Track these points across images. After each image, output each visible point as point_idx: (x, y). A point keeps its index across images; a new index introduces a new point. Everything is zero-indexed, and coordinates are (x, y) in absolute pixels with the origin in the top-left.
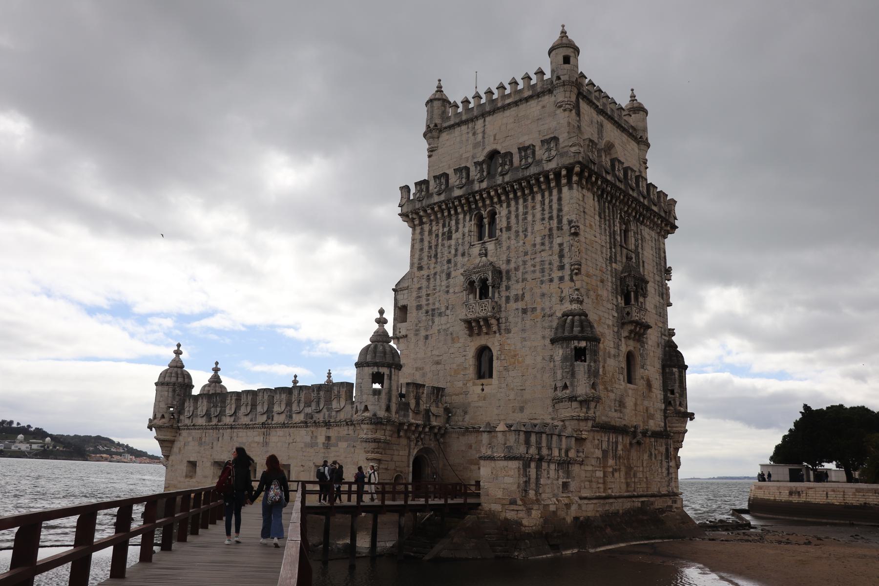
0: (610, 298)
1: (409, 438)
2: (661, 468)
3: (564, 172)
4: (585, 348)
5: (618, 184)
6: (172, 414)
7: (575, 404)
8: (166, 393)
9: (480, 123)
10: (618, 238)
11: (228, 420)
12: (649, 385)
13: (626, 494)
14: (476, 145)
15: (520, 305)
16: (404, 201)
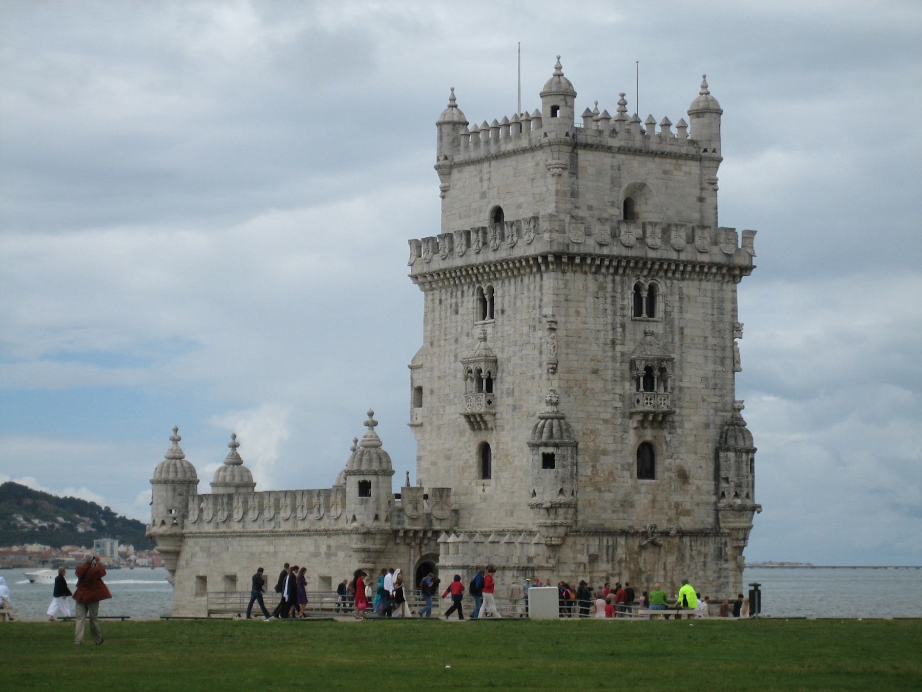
0: (610, 387)
1: (409, 544)
2: (704, 570)
3: (540, 260)
4: (553, 455)
5: (625, 252)
6: (174, 519)
7: (542, 512)
8: (164, 493)
9: (486, 165)
10: (630, 312)
11: (237, 527)
12: (683, 476)
14: (483, 195)
15: (509, 401)
16: (413, 258)
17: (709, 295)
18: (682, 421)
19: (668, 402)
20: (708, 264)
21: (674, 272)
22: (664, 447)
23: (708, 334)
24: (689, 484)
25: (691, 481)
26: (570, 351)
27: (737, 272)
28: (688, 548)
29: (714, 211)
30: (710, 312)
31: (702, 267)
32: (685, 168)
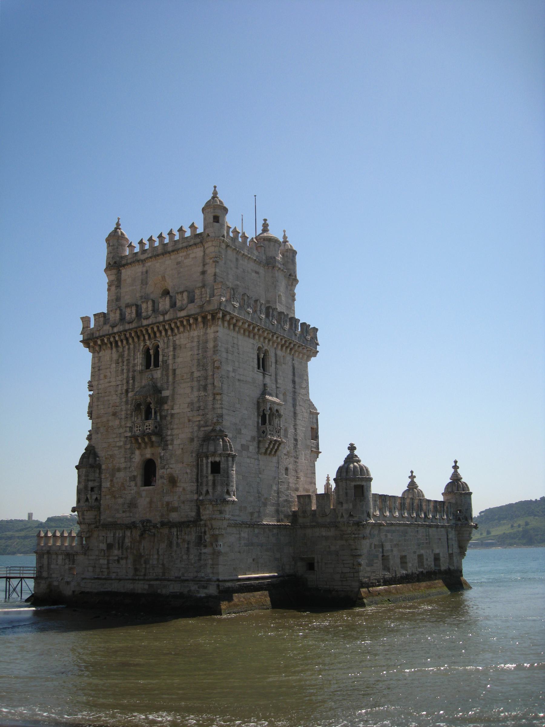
0: (123, 423)
12: (173, 481)
13: (130, 577)
17: (196, 340)
18: (172, 440)
19: (152, 427)
20: (183, 317)
21: (166, 331)
22: (159, 460)
23: (194, 369)
24: (177, 487)
25: (178, 484)
26: (99, 403)
27: (209, 317)
28: (175, 538)
29: (212, 278)
30: (196, 352)
31: (182, 322)
32: (192, 256)
